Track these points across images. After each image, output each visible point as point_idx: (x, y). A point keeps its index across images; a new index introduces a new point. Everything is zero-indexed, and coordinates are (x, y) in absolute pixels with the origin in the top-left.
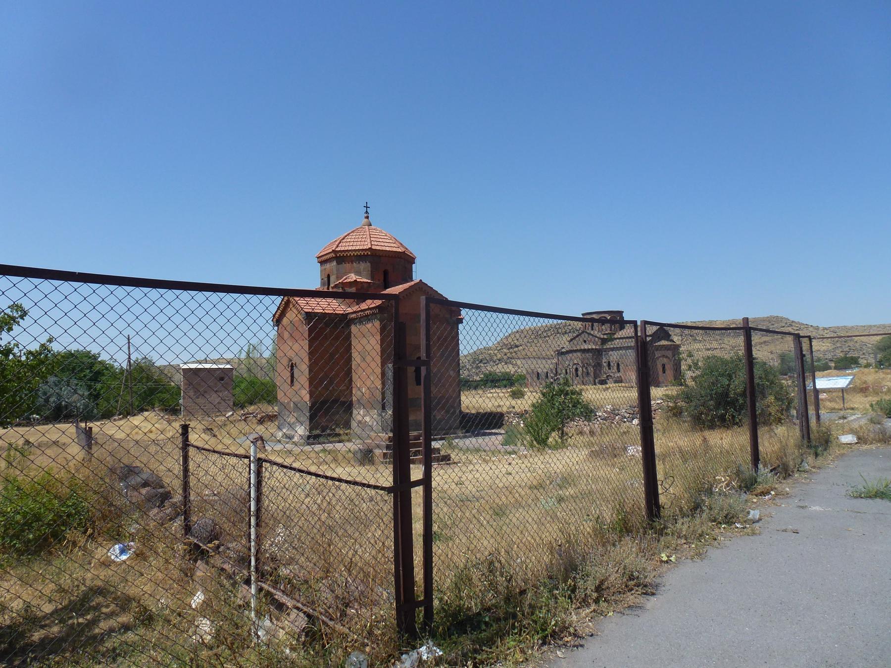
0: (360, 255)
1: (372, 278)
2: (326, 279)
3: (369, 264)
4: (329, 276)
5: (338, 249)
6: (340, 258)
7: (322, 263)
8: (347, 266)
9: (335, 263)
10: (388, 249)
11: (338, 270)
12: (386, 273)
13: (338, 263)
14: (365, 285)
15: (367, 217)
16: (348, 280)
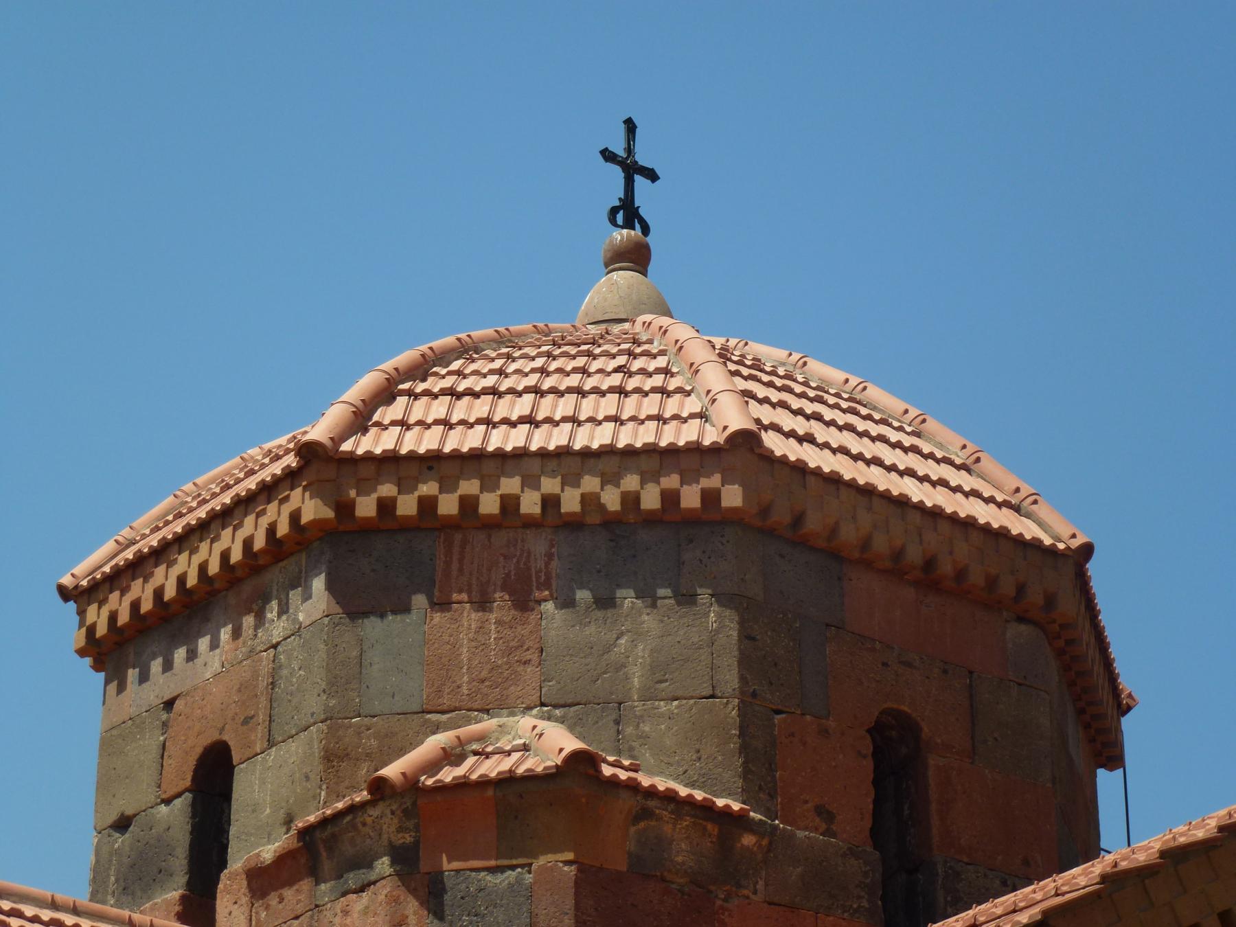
0: (623, 527)
1: (760, 762)
2: (174, 818)
3: (715, 621)
4: (214, 776)
5: (364, 444)
6: (374, 536)
7: (112, 652)
8: (466, 632)
9: (314, 601)
10: (916, 492)
11: (345, 677)
12: (895, 752)
13: (354, 603)
14: (684, 849)
15: (636, 257)
16: (492, 768)
